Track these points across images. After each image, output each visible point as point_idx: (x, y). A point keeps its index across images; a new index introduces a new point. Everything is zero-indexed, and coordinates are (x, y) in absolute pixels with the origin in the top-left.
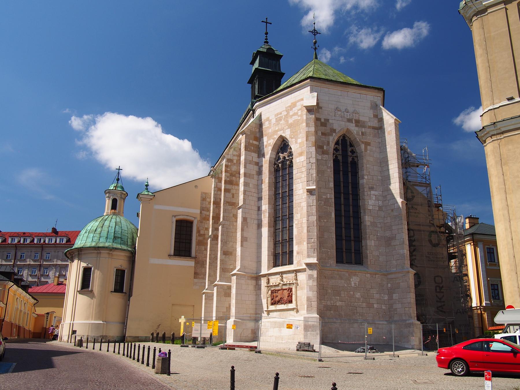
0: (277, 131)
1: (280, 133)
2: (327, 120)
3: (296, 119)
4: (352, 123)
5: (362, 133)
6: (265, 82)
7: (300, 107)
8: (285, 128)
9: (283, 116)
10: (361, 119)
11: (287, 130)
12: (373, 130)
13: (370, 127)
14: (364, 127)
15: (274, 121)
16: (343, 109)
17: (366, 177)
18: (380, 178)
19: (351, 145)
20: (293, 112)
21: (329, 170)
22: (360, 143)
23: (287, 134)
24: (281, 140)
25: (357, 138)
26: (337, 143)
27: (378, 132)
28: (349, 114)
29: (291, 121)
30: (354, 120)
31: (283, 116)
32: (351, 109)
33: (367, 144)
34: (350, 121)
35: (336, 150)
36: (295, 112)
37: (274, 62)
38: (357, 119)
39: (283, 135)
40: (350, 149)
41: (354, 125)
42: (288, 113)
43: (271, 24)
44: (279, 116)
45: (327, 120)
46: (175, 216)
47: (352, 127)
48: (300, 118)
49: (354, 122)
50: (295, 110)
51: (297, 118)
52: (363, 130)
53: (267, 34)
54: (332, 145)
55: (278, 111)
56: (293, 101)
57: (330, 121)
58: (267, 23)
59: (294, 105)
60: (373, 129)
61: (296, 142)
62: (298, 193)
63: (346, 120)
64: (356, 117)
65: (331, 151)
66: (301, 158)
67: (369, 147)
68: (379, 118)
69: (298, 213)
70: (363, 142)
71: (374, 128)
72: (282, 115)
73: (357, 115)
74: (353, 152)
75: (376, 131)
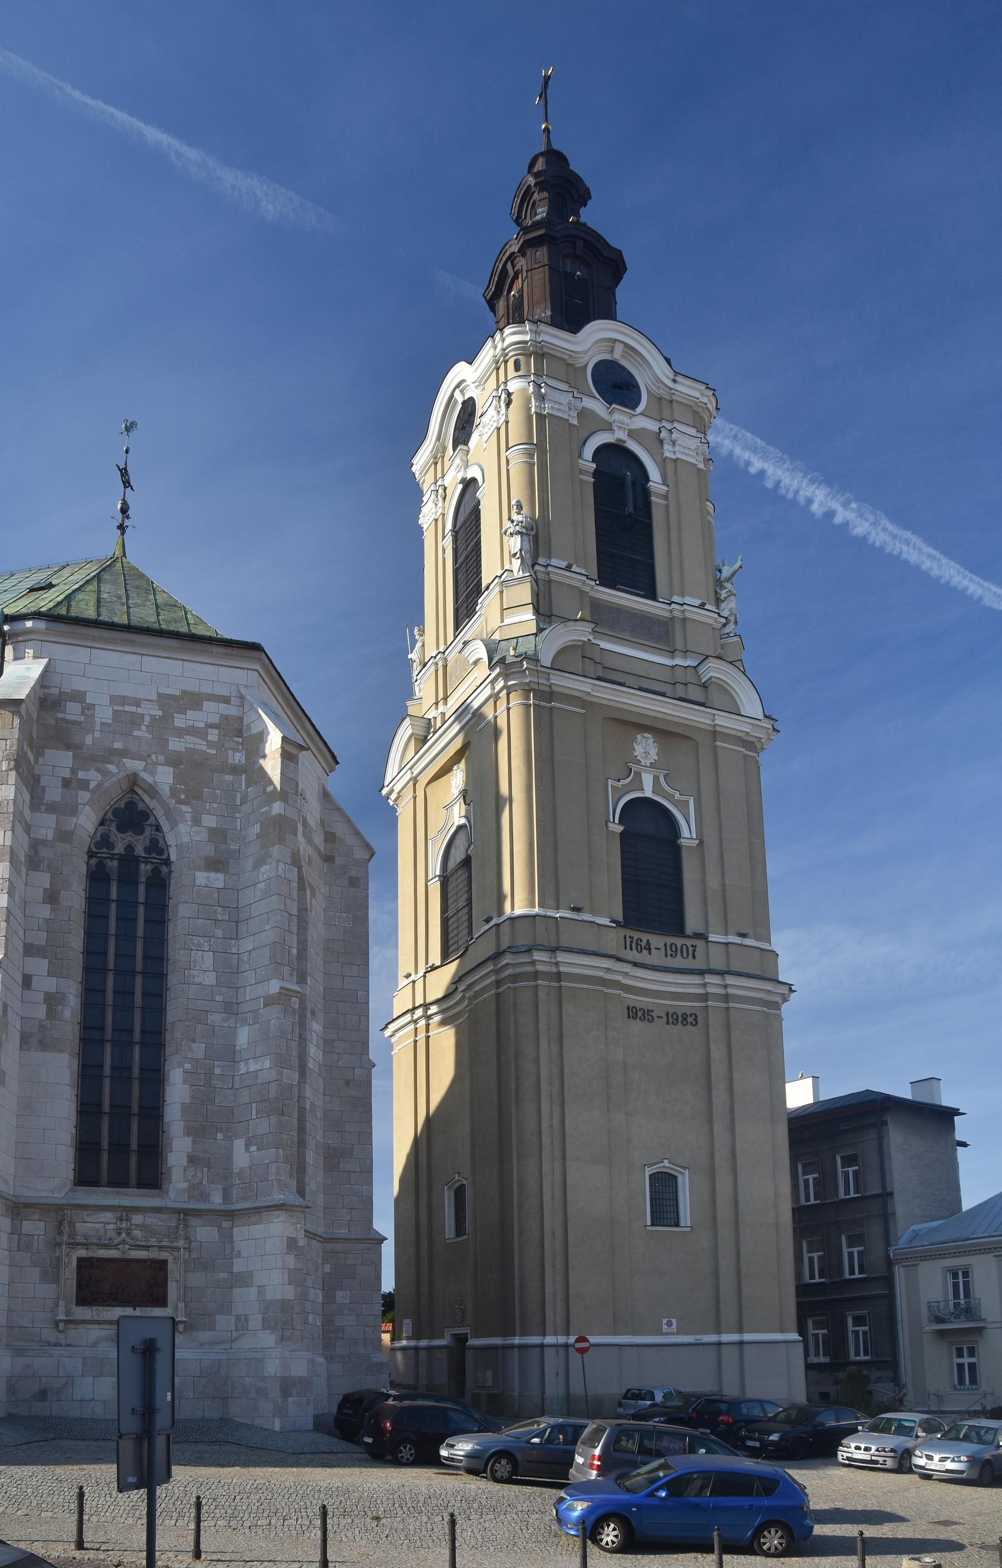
0: (124, 753)
3: (178, 739)
7: (215, 719)
8: (154, 757)
9: (147, 719)
11: (160, 769)
20: (190, 723)
29: (176, 745)
31: (147, 719)
36: (196, 725)
42: (167, 718)
44: (133, 709)
48: (213, 752)
50: (195, 718)
51: (204, 748)
59: (193, 700)
61: (196, 821)
62: (196, 980)
66: (213, 875)
69: (194, 1041)
72: (140, 710)
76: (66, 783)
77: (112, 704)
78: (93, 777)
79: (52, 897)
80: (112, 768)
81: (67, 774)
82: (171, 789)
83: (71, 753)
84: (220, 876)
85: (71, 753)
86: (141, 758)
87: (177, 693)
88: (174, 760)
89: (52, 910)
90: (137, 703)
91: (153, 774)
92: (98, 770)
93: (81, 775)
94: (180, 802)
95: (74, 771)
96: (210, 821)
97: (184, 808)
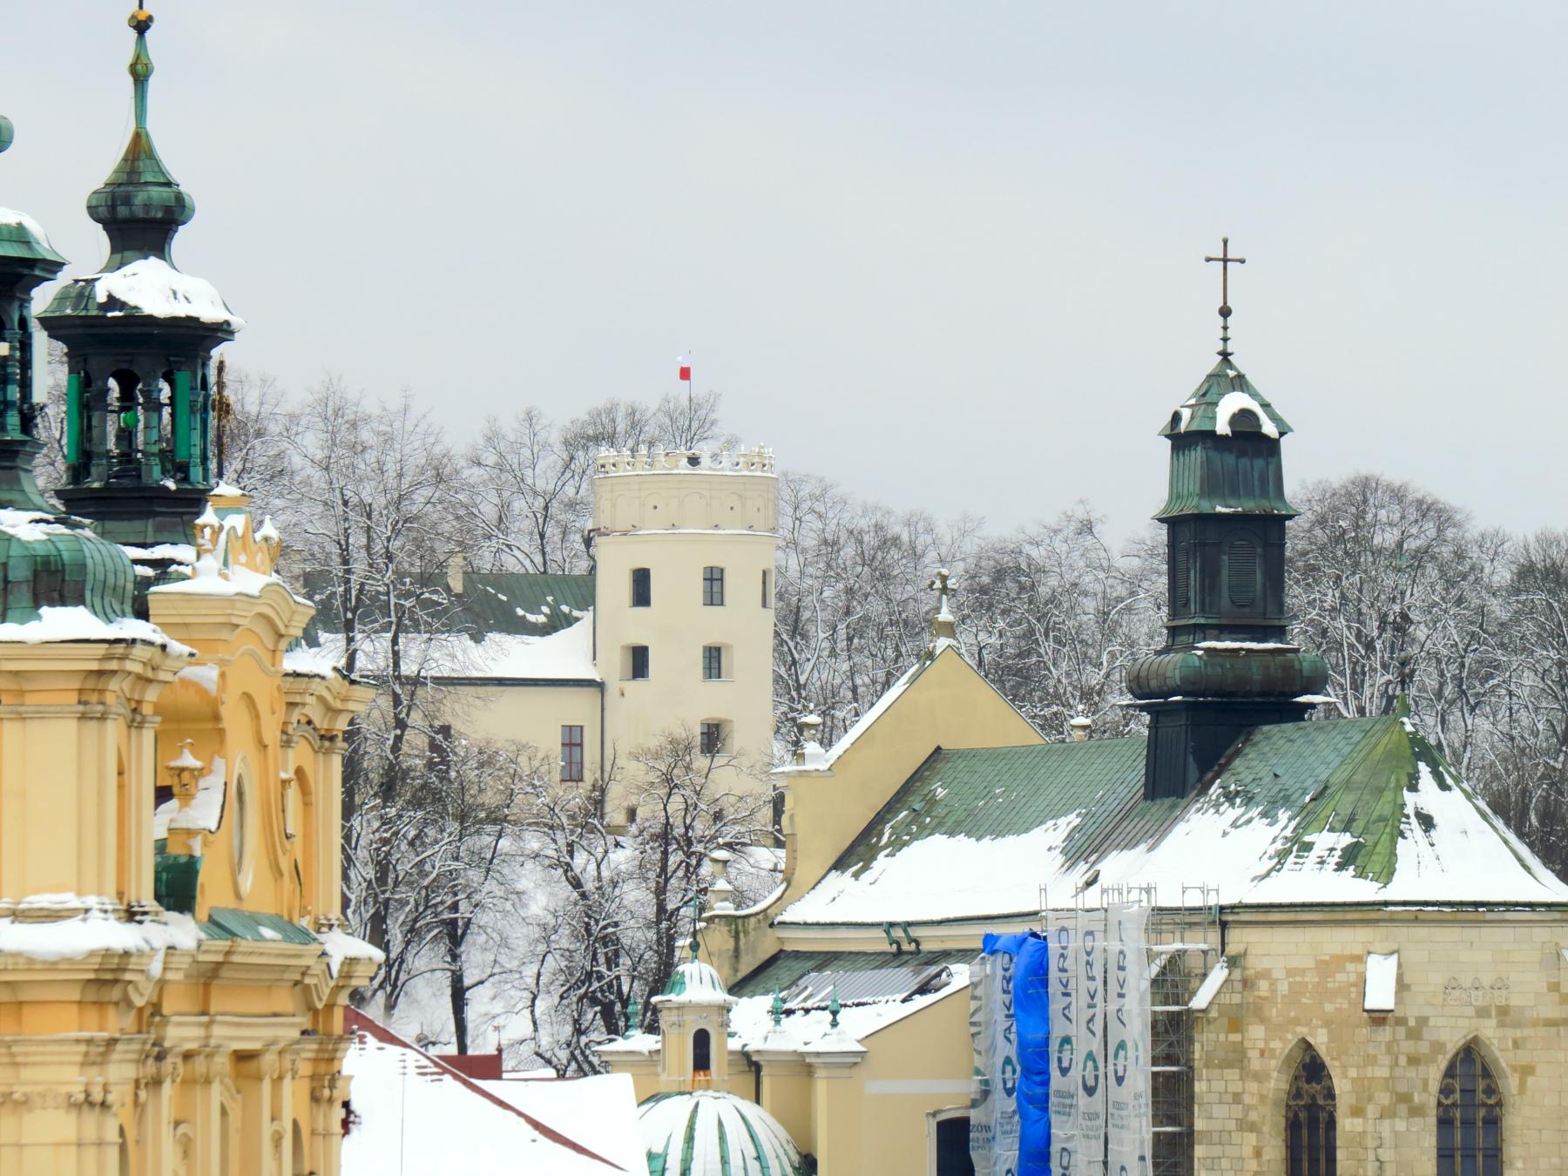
1: (1302, 1031)
2: (1423, 1021)
4: (1490, 1016)
5: (1516, 1044)
6: (1225, 558)
9: (1310, 986)
10: (1515, 1001)
12: (1545, 1028)
13: (1535, 1023)
14: (1517, 1025)
15: (1283, 988)
16: (1466, 981)
17: (1519, 1164)
18: (1556, 1160)
19: (1487, 1074)
21: (1424, 1158)
22: (1508, 1071)
23: (1320, 1040)
24: (1304, 1046)
25: (1501, 1060)
26: (1450, 1073)
27: (1558, 1031)
28: (1480, 993)
30: (1493, 1008)
32: (1487, 979)
33: (1527, 1071)
34: (1482, 1013)
35: (1445, 1091)
37: (1259, 463)
38: (1503, 1003)
39: (1310, 1040)
40: (1481, 1085)
41: (1493, 1022)
43: (1243, 261)
44: (1298, 979)
45: (1423, 1021)
46: (934, 1115)
47: (1489, 1031)
49: (1494, 1013)
52: (1518, 1033)
53: (1225, 312)
54: (1434, 1086)
55: (1296, 963)
56: (1336, 950)
57: (1432, 1022)
58: (1225, 260)
60: (1545, 1025)
61: (1345, 1076)
63: (1471, 1012)
64: (1500, 998)
65: (1433, 1102)
67: (1530, 1080)
68: (1562, 991)
70: (1514, 1069)
71: (1550, 1023)
73: (1503, 993)
74: (1490, 1091)
75: (1554, 1029)
76: (1262, 1053)
77: (1288, 976)
78: (1276, 1044)
79: (1258, 1153)
80: (1289, 1036)
81: (1261, 1045)
82: (1327, 1048)
83: (1263, 1027)
84: (1360, 1121)
85: (1263, 1027)
86: (1306, 1025)
87: (1327, 958)
88: (1327, 1024)
89: (1259, 1165)
90: (1303, 972)
91: (1315, 1037)
92: (1280, 1039)
93: (1273, 1045)
94: (1333, 1059)
95: (1266, 1041)
96: (1353, 1073)
97: (1337, 1063)
